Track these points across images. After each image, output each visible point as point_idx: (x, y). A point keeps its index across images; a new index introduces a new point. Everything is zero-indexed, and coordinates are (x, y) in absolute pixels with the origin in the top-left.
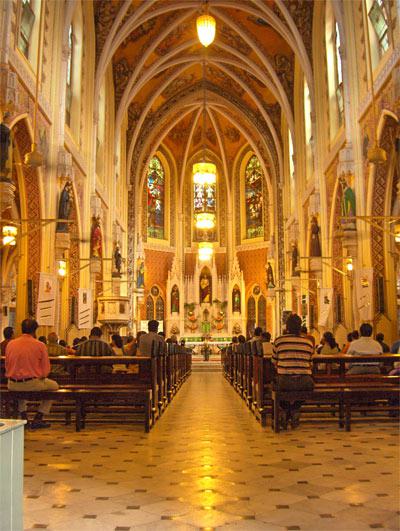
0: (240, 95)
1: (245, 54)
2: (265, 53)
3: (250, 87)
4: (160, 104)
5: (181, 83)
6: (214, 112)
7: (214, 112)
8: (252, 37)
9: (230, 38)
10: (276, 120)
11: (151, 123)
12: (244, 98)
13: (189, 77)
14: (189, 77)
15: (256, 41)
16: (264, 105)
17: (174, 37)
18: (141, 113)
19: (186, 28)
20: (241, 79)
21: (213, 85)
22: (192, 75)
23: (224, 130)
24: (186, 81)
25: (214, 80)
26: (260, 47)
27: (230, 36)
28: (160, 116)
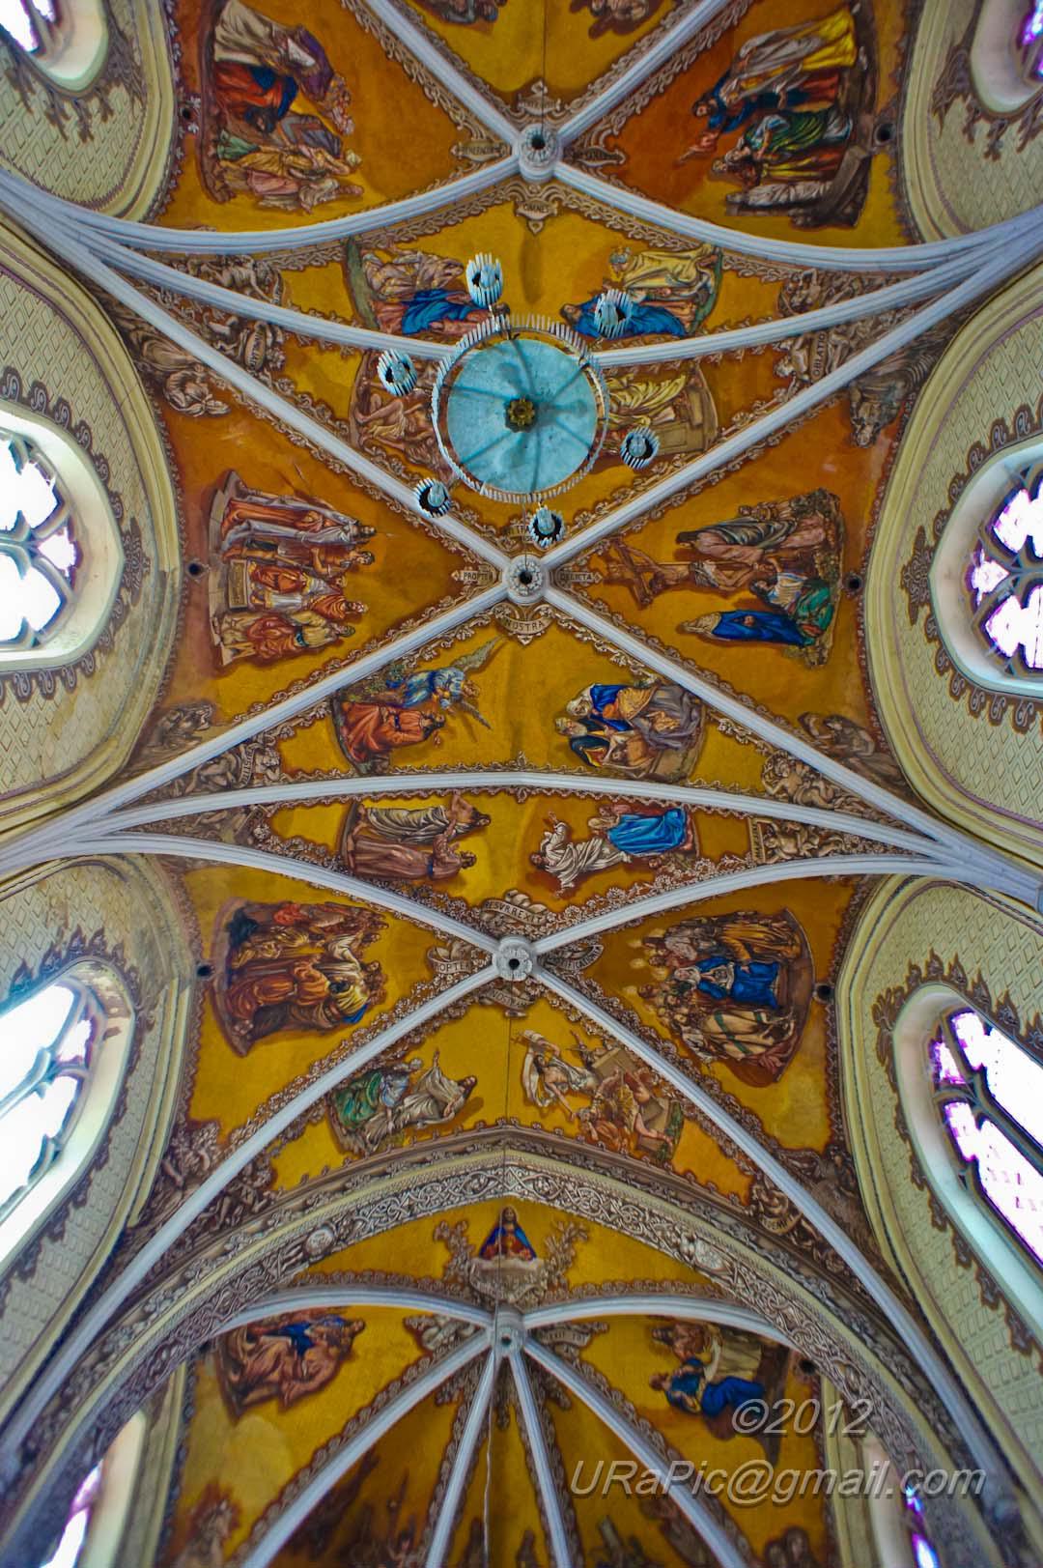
0: (662, 1156)
1: (679, 779)
2: (757, 706)
3: (700, 1082)
4: (315, 1172)
5: (416, 1107)
6: (549, 1393)
7: (549, 1393)
8: (699, 672)
9: (618, 738)
10: (843, 1209)
11: (256, 1225)
12: (679, 1163)
13: (451, 1092)
14: (451, 1092)
15: (719, 683)
16: (775, 1149)
17: (414, 720)
18: (223, 1158)
19: (457, 700)
20: (666, 1054)
21: (545, 1142)
22: (467, 1087)
23: (590, 1541)
24: (440, 1104)
25: (557, 1118)
26: (737, 695)
27: (621, 724)
28: (305, 1207)
